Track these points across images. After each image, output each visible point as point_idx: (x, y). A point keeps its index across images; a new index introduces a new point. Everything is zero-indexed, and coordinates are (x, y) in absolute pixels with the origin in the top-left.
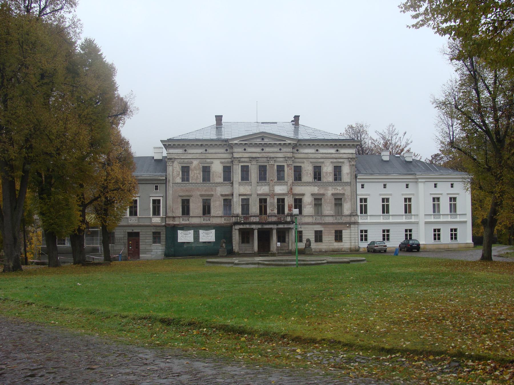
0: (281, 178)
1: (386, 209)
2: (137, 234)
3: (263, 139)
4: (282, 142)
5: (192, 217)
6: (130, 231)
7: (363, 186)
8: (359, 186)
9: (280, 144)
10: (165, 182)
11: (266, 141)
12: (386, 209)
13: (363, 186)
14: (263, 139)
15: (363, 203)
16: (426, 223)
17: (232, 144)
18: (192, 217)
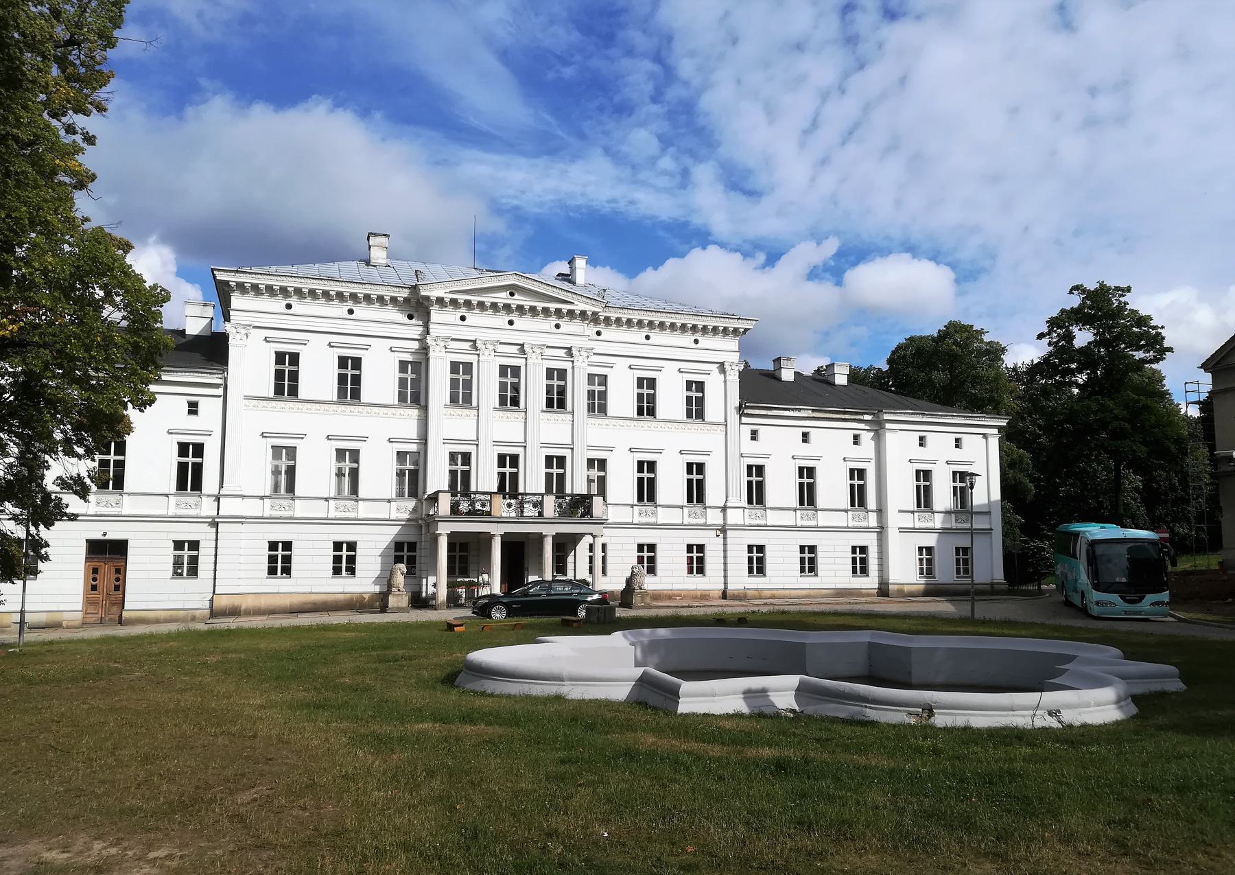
0: (557, 400)
1: (807, 495)
2: (120, 548)
3: (512, 294)
4: (565, 307)
5: (300, 498)
6: (98, 536)
7: (754, 435)
8: (746, 431)
10: (220, 391)
11: (518, 300)
12: (807, 495)
13: (754, 435)
14: (512, 294)
15: (754, 479)
16: (902, 530)
17: (428, 298)
18: (300, 498)
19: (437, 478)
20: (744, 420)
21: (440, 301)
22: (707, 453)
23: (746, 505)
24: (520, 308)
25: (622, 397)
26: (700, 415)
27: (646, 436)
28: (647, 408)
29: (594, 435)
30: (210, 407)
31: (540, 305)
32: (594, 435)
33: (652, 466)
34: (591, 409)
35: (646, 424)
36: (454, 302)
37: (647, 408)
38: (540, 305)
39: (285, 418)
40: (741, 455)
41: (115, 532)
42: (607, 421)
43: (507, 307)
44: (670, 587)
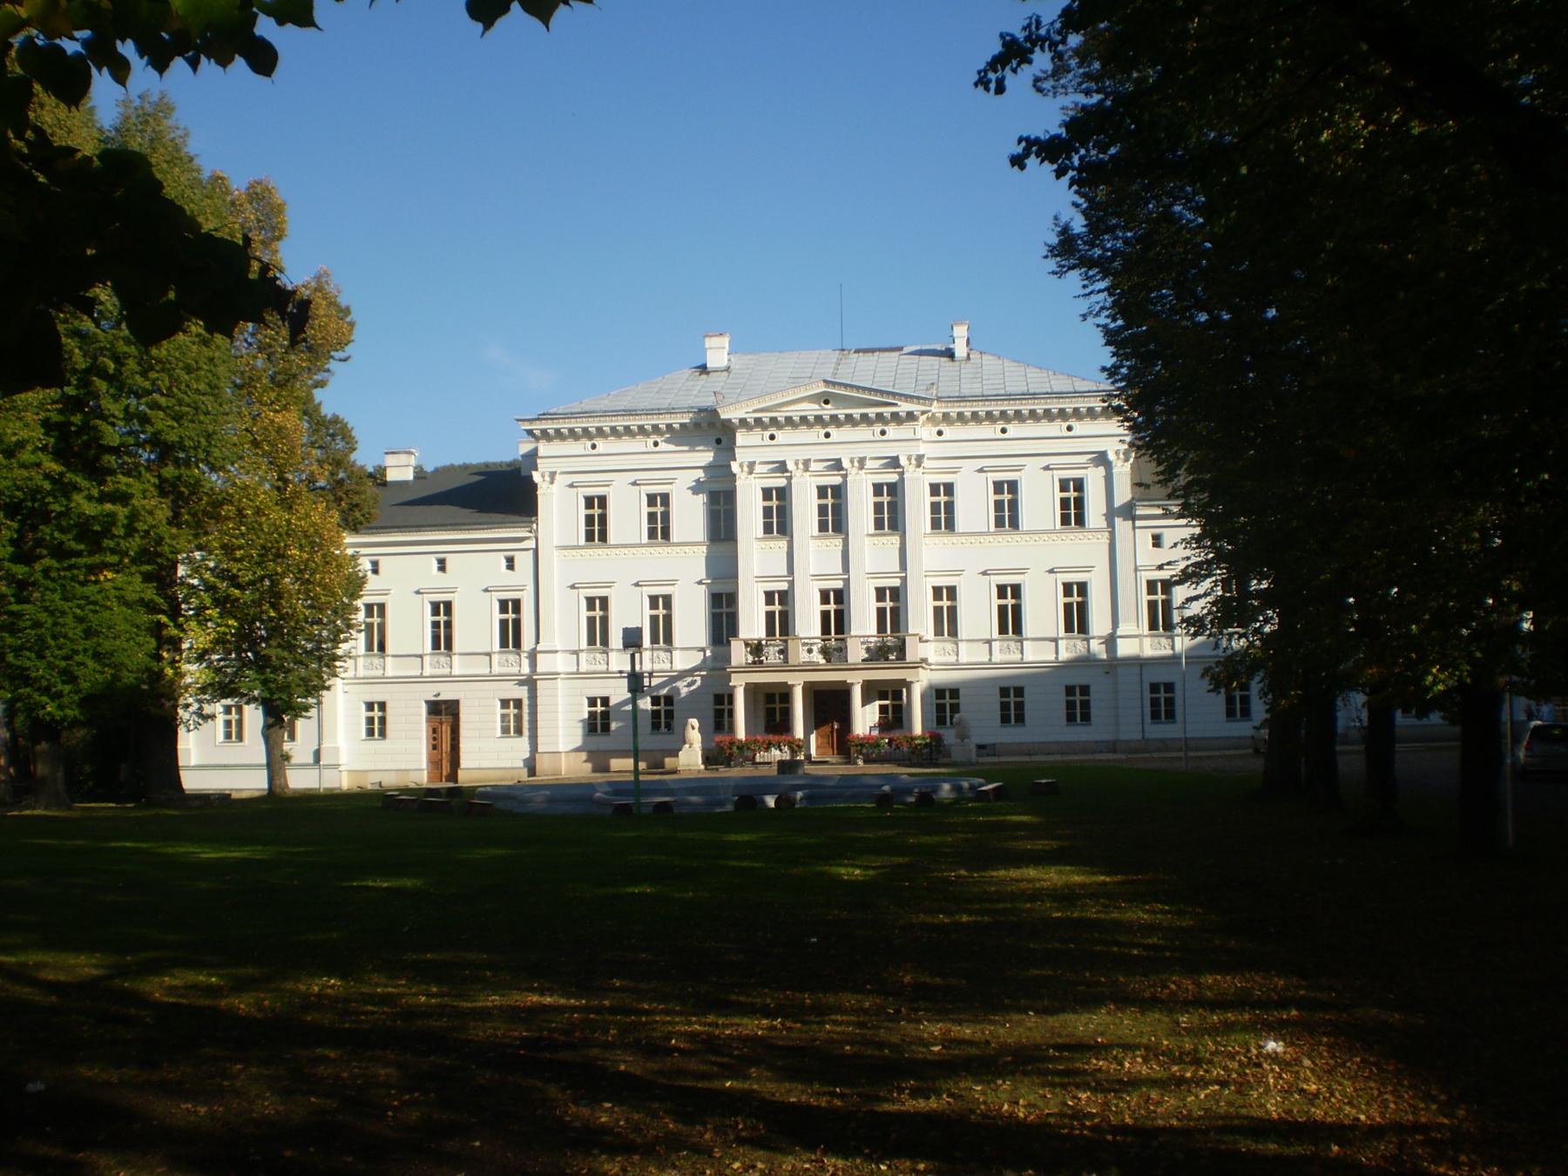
4: (887, 411)
9: (880, 416)
19: (752, 622)
20: (1138, 523)
21: (743, 422)
22: (1088, 569)
23: (1146, 631)
24: (834, 420)
25: (975, 505)
26: (1080, 521)
27: (1007, 553)
28: (1007, 515)
29: (931, 558)
30: (524, 561)
31: (856, 412)
32: (931, 558)
33: (1016, 590)
34: (935, 524)
35: (1008, 539)
36: (759, 422)
37: (1007, 515)
38: (856, 412)
39: (597, 565)
40: (1136, 570)
41: (447, 695)
42: (954, 539)
43: (819, 420)
44: (1043, 739)
